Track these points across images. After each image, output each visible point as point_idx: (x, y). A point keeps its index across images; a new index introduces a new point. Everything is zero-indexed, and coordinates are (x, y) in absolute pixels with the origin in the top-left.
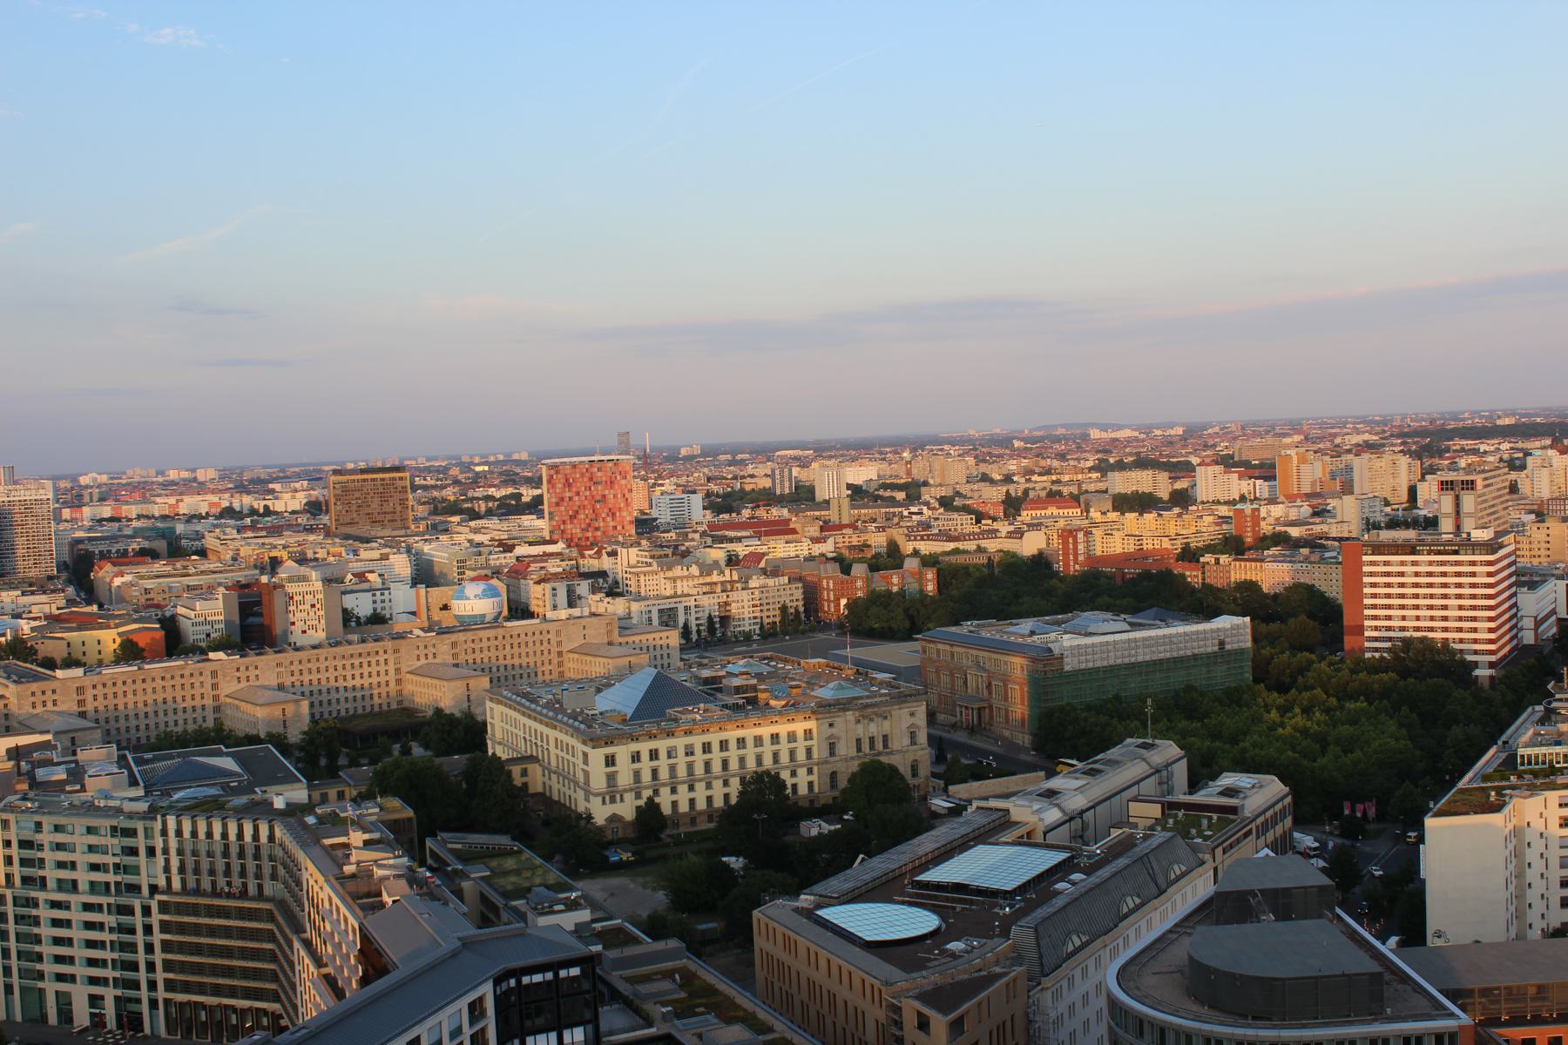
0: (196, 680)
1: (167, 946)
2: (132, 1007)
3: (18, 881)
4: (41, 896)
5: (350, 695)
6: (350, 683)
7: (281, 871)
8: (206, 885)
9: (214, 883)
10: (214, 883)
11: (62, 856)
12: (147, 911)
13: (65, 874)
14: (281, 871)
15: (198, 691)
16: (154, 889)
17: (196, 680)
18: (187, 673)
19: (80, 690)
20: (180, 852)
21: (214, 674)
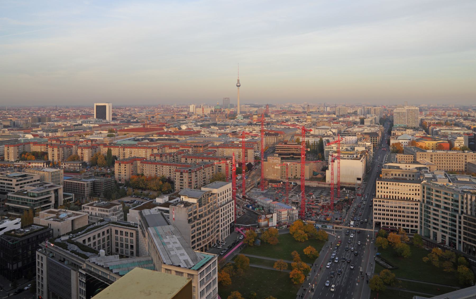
0: (461, 157)
1: (465, 228)
2: (454, 241)
3: (425, 202)
4: (431, 207)
11: (437, 198)
13: (438, 203)
15: (461, 160)
17: (461, 157)
18: (458, 155)
19: (432, 156)
21: (466, 156)
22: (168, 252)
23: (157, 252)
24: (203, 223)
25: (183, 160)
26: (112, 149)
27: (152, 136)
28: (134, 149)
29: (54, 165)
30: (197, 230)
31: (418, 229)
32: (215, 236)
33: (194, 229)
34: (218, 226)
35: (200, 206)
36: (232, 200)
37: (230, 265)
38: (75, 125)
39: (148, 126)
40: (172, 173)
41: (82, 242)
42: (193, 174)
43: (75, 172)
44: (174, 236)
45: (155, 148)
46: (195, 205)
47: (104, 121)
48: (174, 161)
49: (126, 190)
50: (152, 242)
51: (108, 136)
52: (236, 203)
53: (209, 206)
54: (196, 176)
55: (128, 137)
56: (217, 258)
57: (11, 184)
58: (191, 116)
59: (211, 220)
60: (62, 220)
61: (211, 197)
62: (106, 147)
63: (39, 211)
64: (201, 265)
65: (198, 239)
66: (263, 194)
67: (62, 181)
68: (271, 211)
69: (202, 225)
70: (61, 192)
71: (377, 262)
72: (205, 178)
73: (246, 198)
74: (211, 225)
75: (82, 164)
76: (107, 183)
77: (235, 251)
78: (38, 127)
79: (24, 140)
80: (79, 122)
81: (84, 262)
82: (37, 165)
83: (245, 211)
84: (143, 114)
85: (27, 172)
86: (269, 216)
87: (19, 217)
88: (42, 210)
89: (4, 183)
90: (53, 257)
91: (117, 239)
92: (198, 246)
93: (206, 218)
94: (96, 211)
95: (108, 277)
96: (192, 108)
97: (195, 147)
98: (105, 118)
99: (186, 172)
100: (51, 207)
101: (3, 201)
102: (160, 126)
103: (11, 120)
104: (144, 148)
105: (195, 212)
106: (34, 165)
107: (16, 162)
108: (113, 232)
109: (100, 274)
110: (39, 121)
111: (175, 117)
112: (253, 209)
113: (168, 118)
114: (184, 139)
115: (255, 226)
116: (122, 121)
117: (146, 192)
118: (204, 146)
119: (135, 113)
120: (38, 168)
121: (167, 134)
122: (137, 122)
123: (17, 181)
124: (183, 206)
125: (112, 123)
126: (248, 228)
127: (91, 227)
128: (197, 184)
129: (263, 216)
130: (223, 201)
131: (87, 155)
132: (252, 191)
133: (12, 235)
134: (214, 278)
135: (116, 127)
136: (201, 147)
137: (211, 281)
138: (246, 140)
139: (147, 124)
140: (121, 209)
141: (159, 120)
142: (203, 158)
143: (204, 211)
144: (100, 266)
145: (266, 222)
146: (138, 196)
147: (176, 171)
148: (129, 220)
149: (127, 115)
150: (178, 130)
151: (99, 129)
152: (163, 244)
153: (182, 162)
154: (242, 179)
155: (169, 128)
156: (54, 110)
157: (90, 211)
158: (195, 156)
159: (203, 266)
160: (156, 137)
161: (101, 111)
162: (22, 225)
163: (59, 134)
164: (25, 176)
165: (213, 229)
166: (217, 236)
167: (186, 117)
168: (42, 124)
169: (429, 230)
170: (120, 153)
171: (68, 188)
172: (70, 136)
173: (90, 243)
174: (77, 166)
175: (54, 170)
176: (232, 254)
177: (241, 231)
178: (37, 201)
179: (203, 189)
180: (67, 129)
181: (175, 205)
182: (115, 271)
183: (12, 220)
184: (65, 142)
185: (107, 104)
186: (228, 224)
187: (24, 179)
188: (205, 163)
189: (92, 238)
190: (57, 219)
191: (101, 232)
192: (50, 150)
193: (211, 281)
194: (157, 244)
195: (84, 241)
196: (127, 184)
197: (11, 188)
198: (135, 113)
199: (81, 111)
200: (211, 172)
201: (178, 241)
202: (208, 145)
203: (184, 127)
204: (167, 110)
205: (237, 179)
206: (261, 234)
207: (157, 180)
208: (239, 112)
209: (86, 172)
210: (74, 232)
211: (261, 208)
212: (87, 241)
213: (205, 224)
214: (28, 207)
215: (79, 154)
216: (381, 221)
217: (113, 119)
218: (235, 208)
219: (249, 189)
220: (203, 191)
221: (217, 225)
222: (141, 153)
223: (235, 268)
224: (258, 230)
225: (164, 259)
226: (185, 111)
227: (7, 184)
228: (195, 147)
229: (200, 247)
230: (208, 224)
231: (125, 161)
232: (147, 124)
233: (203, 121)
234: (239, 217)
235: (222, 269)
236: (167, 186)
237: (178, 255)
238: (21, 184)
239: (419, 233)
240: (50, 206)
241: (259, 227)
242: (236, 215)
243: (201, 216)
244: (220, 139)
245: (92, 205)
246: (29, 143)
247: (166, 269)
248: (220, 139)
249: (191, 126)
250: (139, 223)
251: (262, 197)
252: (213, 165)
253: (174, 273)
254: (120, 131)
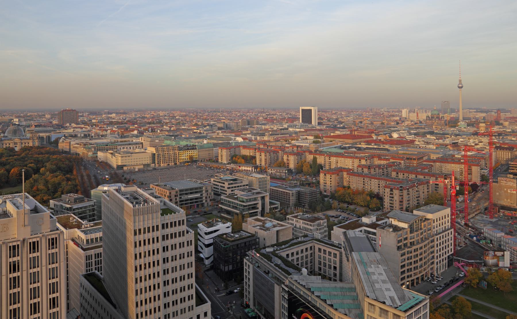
22: (372, 284)
23: (360, 281)
24: (415, 251)
25: (394, 174)
26: (317, 156)
27: (360, 144)
28: (341, 159)
29: (262, 171)
30: (408, 259)
32: (429, 268)
33: (404, 257)
34: (433, 257)
35: (411, 232)
36: (451, 228)
37: (447, 308)
38: (281, 129)
39: (356, 133)
40: (381, 188)
41: (285, 256)
42: (405, 192)
43: (281, 179)
44: (380, 266)
45: (363, 158)
46: (405, 231)
47: (310, 126)
48: (383, 173)
49: (332, 202)
50: (356, 268)
51: (314, 142)
52: (455, 231)
53: (422, 234)
54: (408, 194)
55: (334, 144)
56: (428, 300)
57: (224, 187)
58: (403, 122)
59: (424, 249)
60: (268, 229)
61: (425, 223)
62: (311, 154)
63: (247, 217)
64: (409, 306)
65: (408, 270)
66: (491, 222)
67: (268, 187)
68: (502, 247)
69: (413, 254)
70: (267, 200)
72: (419, 197)
73: (469, 226)
74: (424, 255)
75: (288, 170)
76: (311, 193)
77: (454, 290)
78: (247, 130)
79: (235, 143)
80: (286, 126)
81: (287, 278)
82: (246, 168)
83: (467, 241)
84: (351, 118)
85: (237, 176)
86: (499, 254)
87: (230, 221)
88: (251, 216)
89: (218, 186)
90: (258, 267)
91: (320, 257)
92: (408, 277)
93: (418, 246)
94: (300, 224)
95: (310, 299)
96: (404, 113)
97: (408, 159)
98: (311, 123)
99: (396, 189)
101: (217, 202)
102: (369, 133)
103: (224, 122)
104: (351, 157)
105: (406, 239)
106: (243, 168)
107: (228, 164)
108: (317, 250)
109: (302, 293)
110: (248, 124)
111: (385, 122)
112: (478, 240)
113: (378, 124)
114: (395, 149)
115: (481, 263)
116: (328, 126)
117: (352, 207)
118: (419, 159)
119: (342, 117)
120: (247, 172)
121: (377, 142)
122: (344, 128)
123: (229, 184)
124: (391, 230)
125: (318, 128)
126: (471, 264)
127: (295, 241)
128: (409, 204)
129: (491, 253)
130: (440, 229)
131: (292, 162)
132: (477, 217)
133: (223, 238)
135: (322, 132)
136: (415, 159)
138: (469, 153)
139: (355, 130)
140: (325, 224)
141: (367, 126)
142: (417, 174)
143: (416, 239)
144: (302, 285)
145: (495, 261)
146: (343, 210)
147: (386, 187)
148: (333, 239)
149: (333, 119)
150: (388, 138)
151: (305, 134)
152: (367, 273)
153: (393, 176)
154: (464, 201)
155: (379, 135)
156: (262, 112)
157: (294, 222)
158: (408, 170)
159: (411, 308)
160: (363, 146)
161: (307, 115)
162: (233, 229)
163: (266, 138)
164: (235, 180)
165: (426, 260)
166: (432, 269)
167: (398, 123)
168: (251, 127)
170: (326, 163)
171: (274, 196)
172: (277, 140)
173: (293, 258)
174: (283, 172)
175: (261, 176)
176: (449, 293)
177: (461, 267)
178: (246, 206)
179: (415, 212)
180: (274, 133)
181: (383, 228)
182: (316, 293)
183: (224, 223)
184: (272, 146)
185: (312, 108)
186: (445, 256)
187: (235, 183)
188: (419, 180)
189: (295, 254)
190: (263, 228)
191: (304, 248)
192: (258, 155)
194: (360, 272)
195: (288, 255)
196: (333, 196)
197: (224, 190)
198: (342, 117)
199: (287, 114)
200: (426, 190)
201: (384, 273)
202: (422, 158)
203: (395, 135)
204: (376, 114)
205: (458, 201)
206: (487, 274)
207: (364, 196)
208: (461, 118)
209: (292, 180)
210: (278, 244)
211: (489, 242)
212: (290, 255)
213: (416, 253)
214: (238, 212)
215: (285, 160)
217: (319, 124)
218: (455, 236)
219: (474, 215)
220: (415, 215)
221: (431, 256)
222: (348, 163)
223: (453, 312)
224: (484, 269)
225: (367, 291)
226: (396, 116)
227: (220, 186)
228: (408, 159)
229: (410, 279)
230: (421, 254)
231: (331, 172)
232: (355, 130)
233: (418, 128)
234: (459, 248)
235: (436, 310)
236: (375, 203)
237: (384, 289)
238: (232, 187)
241: (485, 265)
242: (455, 245)
243: (412, 244)
244: (438, 151)
245: (296, 217)
246: (239, 147)
247: (369, 304)
248: (438, 151)
249: (403, 133)
250: (342, 243)
251: (489, 227)
252: (428, 182)
253: (378, 310)
254: (326, 137)
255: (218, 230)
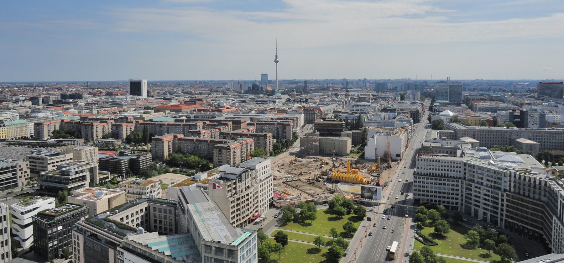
2: (496, 219)
5: (551, 144)
6: (552, 141)
7: (548, 194)
8: (522, 192)
9: (524, 193)
10: (524, 193)
12: (502, 195)
13: (480, 180)
14: (548, 194)
16: (505, 190)
20: (514, 182)
31: (459, 205)
34: (258, 201)
41: (119, 220)
44: (214, 212)
71: (416, 238)
89: (36, 163)
92: (237, 221)
100: (86, 185)
134: (254, 253)
137: (251, 256)
144: (138, 243)
169: (470, 207)
189: (130, 216)
193: (251, 256)
195: (122, 219)
201: (218, 217)
212: (125, 218)
216: (421, 197)
227: (39, 163)
229: (239, 222)
239: (459, 209)
240: (84, 184)
255: (37, 208)
